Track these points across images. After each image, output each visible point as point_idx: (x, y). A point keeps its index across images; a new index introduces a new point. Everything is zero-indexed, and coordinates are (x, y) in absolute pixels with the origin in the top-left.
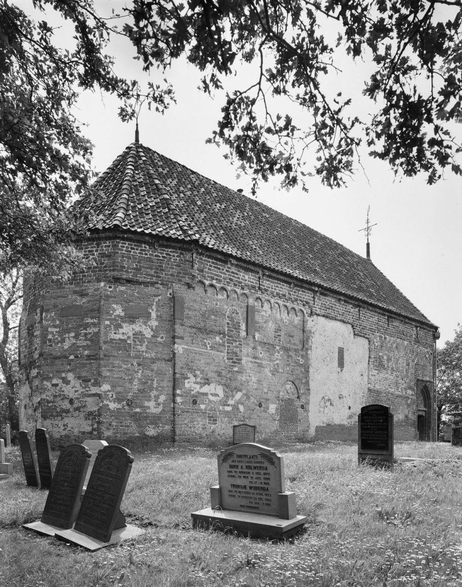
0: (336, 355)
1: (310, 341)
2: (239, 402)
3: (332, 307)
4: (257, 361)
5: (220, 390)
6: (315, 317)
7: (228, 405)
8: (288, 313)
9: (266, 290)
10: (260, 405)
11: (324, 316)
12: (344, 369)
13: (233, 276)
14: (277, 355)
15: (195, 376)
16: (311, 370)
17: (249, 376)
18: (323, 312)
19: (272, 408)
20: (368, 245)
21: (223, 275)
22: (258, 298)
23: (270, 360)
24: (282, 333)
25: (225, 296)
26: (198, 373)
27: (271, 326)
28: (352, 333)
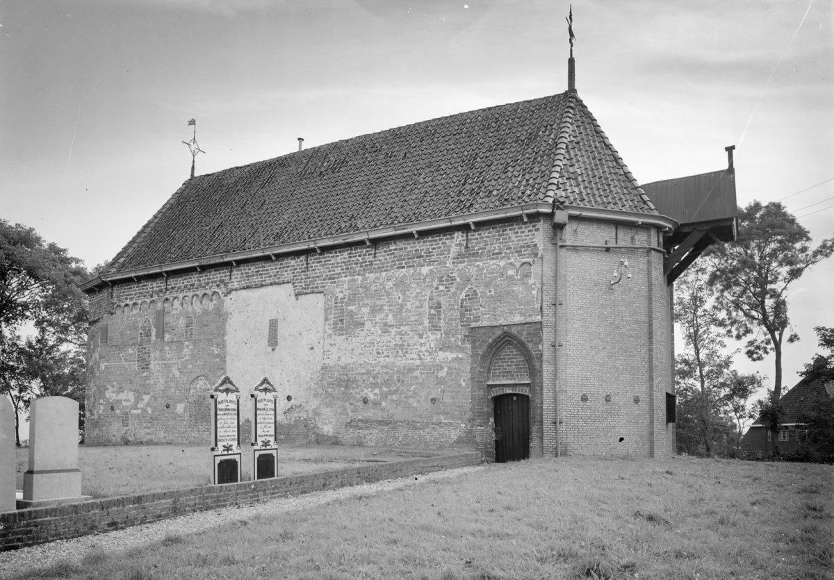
0: (266, 331)
1: (227, 325)
2: (148, 405)
3: (259, 271)
4: (165, 362)
5: (131, 396)
6: (233, 293)
7: (138, 409)
8: (201, 302)
9: (173, 288)
10: (168, 407)
11: (244, 288)
12: (277, 348)
13: (143, 289)
14: (186, 351)
15: (113, 387)
16: (228, 359)
17: (157, 379)
18: (243, 284)
19: (180, 408)
20: (571, 62)
21: (133, 293)
22: (167, 299)
23: (179, 358)
24: (194, 326)
25: (138, 310)
26: (115, 383)
27: (182, 322)
28: (293, 294)
